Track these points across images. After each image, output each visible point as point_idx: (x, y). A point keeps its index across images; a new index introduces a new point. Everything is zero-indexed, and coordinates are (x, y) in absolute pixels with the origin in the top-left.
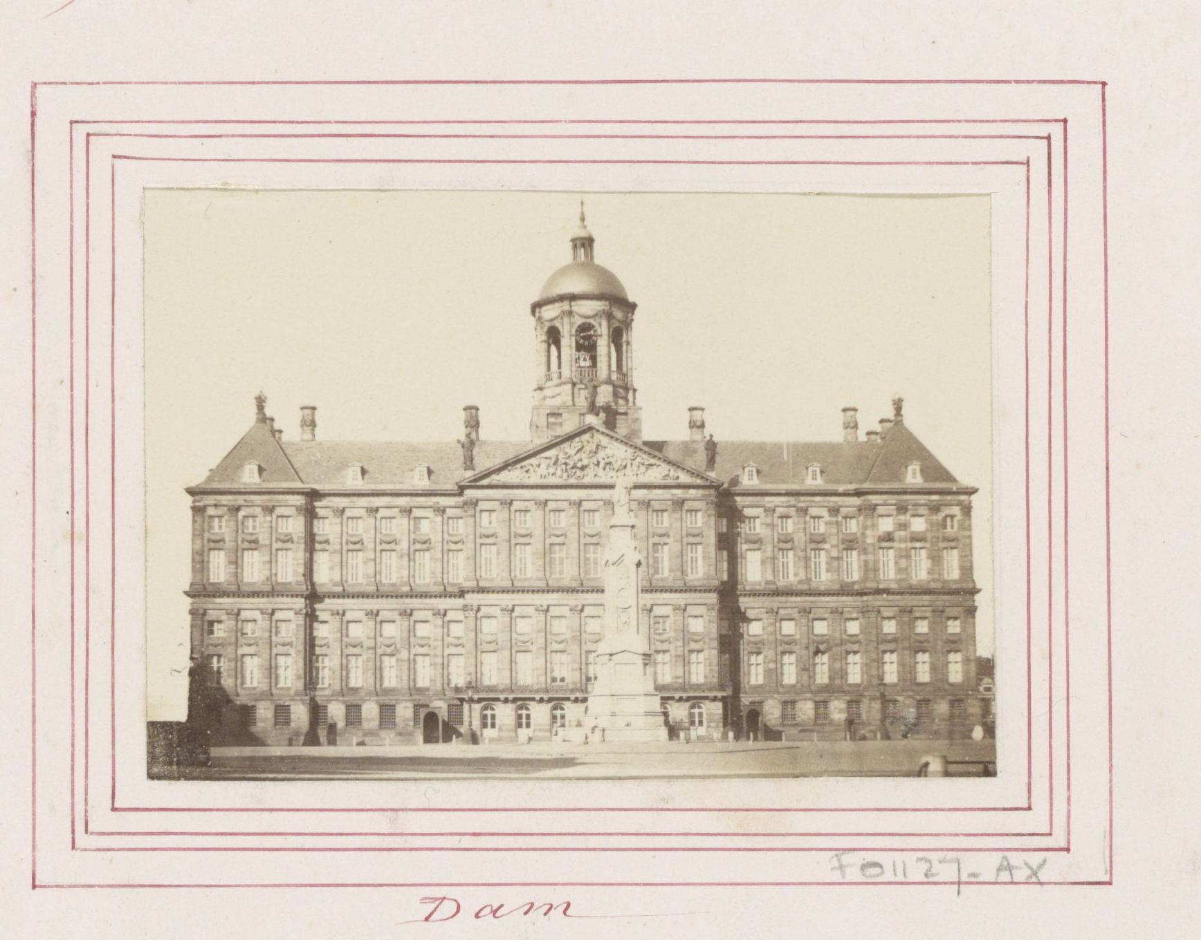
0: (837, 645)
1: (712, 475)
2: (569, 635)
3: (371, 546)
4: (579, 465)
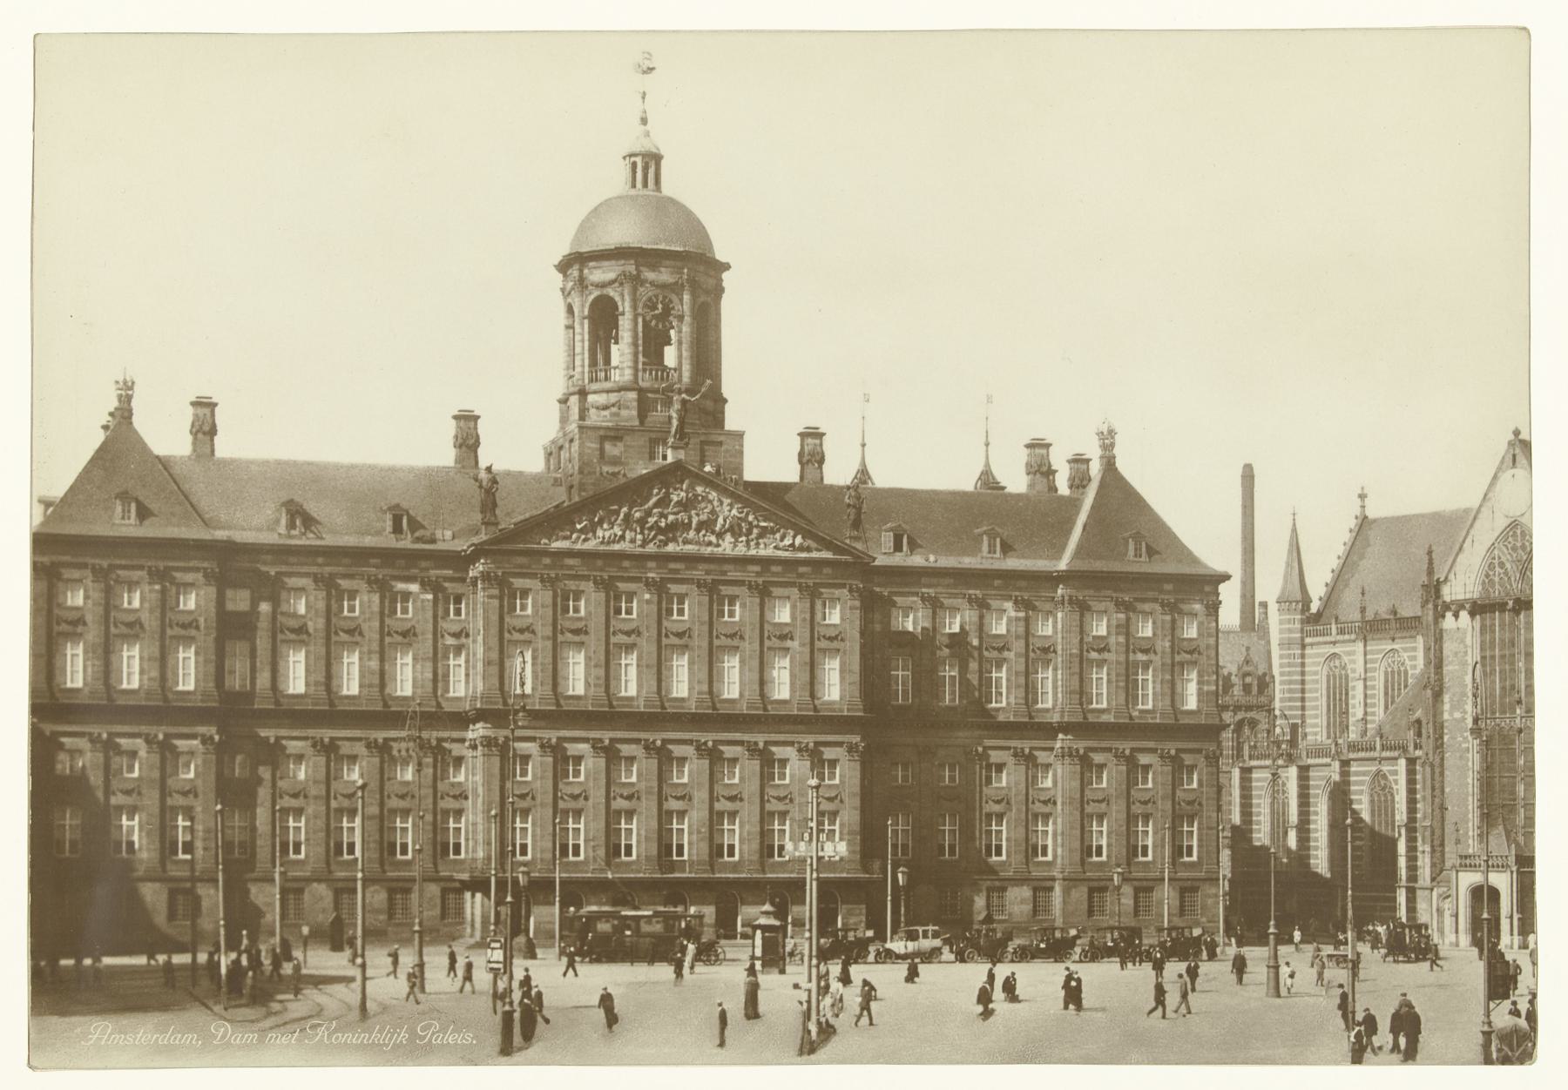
2: (643, 785)
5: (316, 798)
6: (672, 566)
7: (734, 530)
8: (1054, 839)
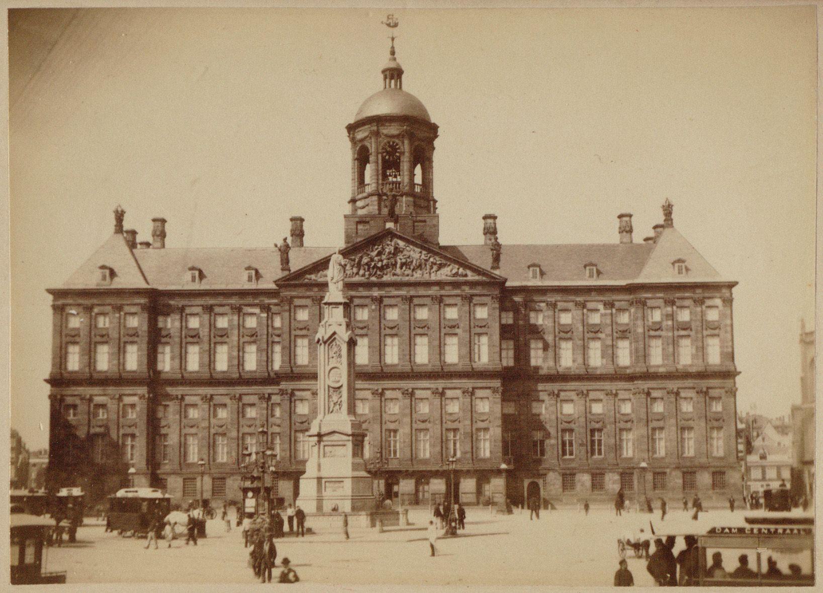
0: (610, 424)
1: (497, 272)
2: (371, 416)
3: (206, 339)
4: (379, 265)
6: (387, 289)
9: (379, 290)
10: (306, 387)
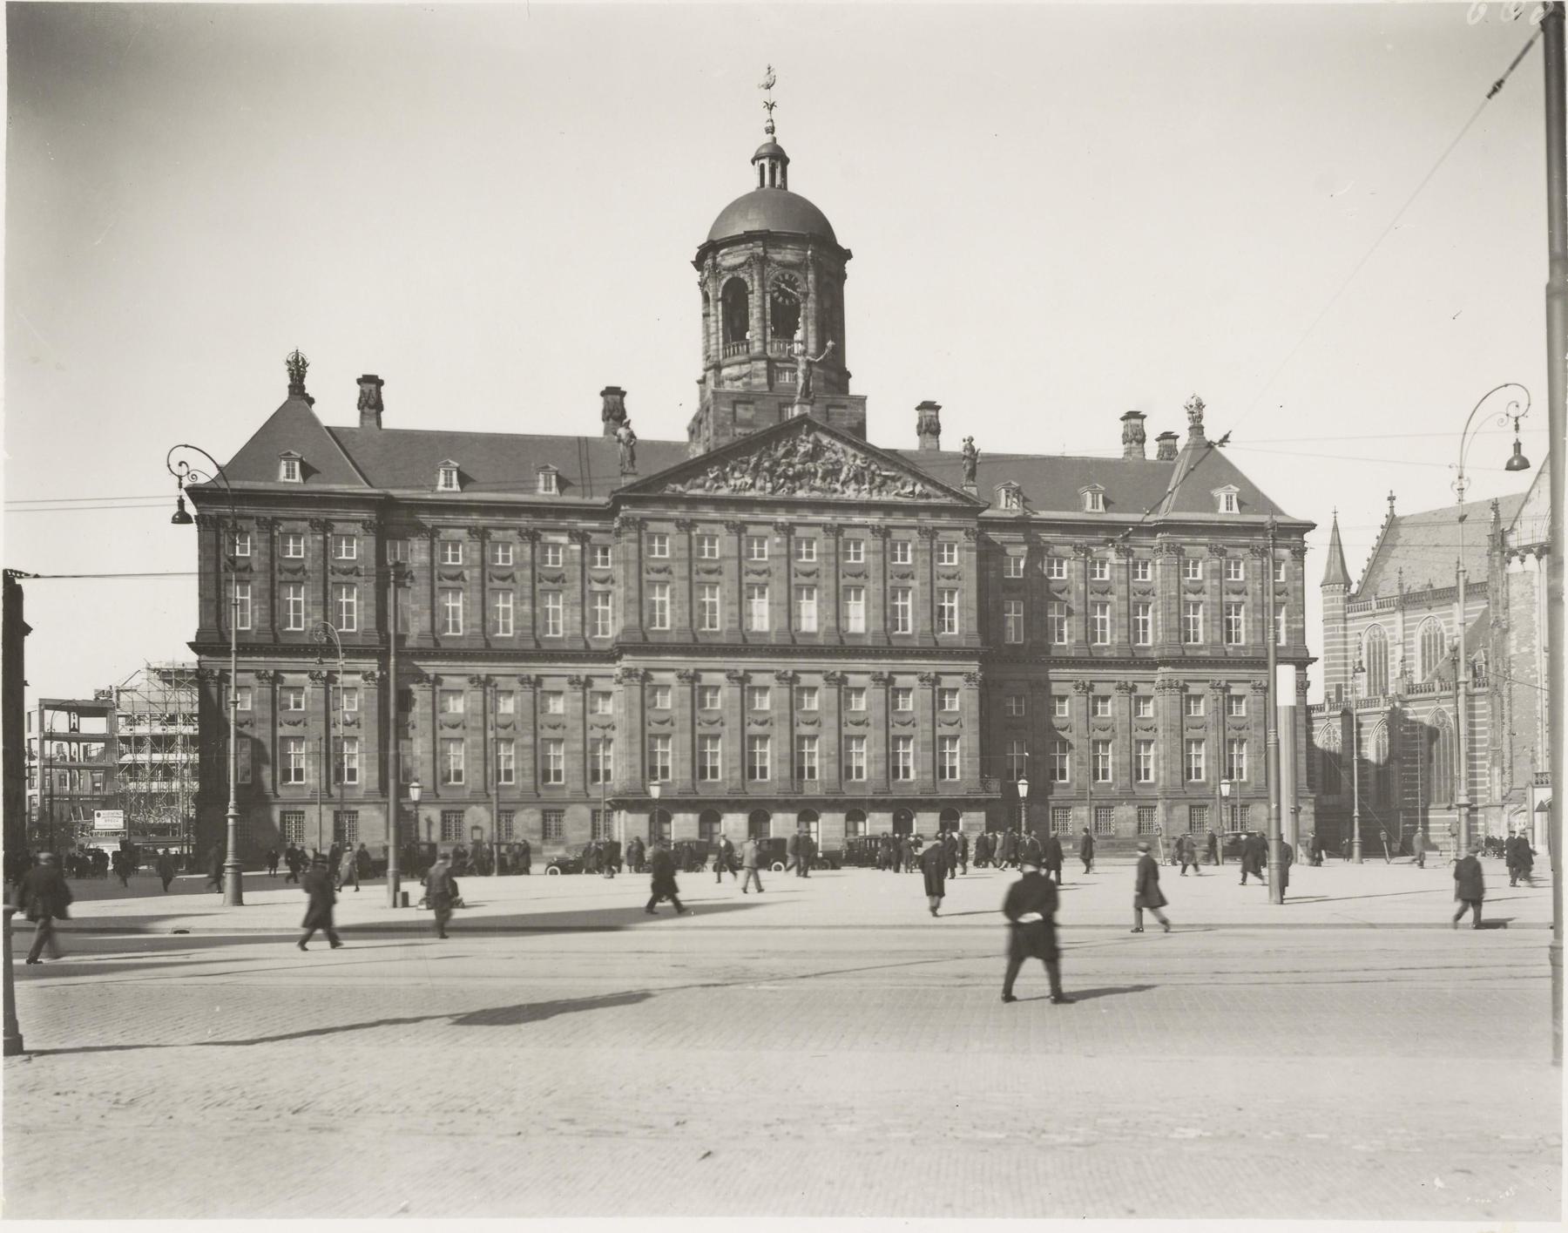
2: (775, 713)
4: (790, 473)
5: (474, 729)
7: (858, 478)
8: (1155, 763)
9: (788, 512)
10: (670, 665)
